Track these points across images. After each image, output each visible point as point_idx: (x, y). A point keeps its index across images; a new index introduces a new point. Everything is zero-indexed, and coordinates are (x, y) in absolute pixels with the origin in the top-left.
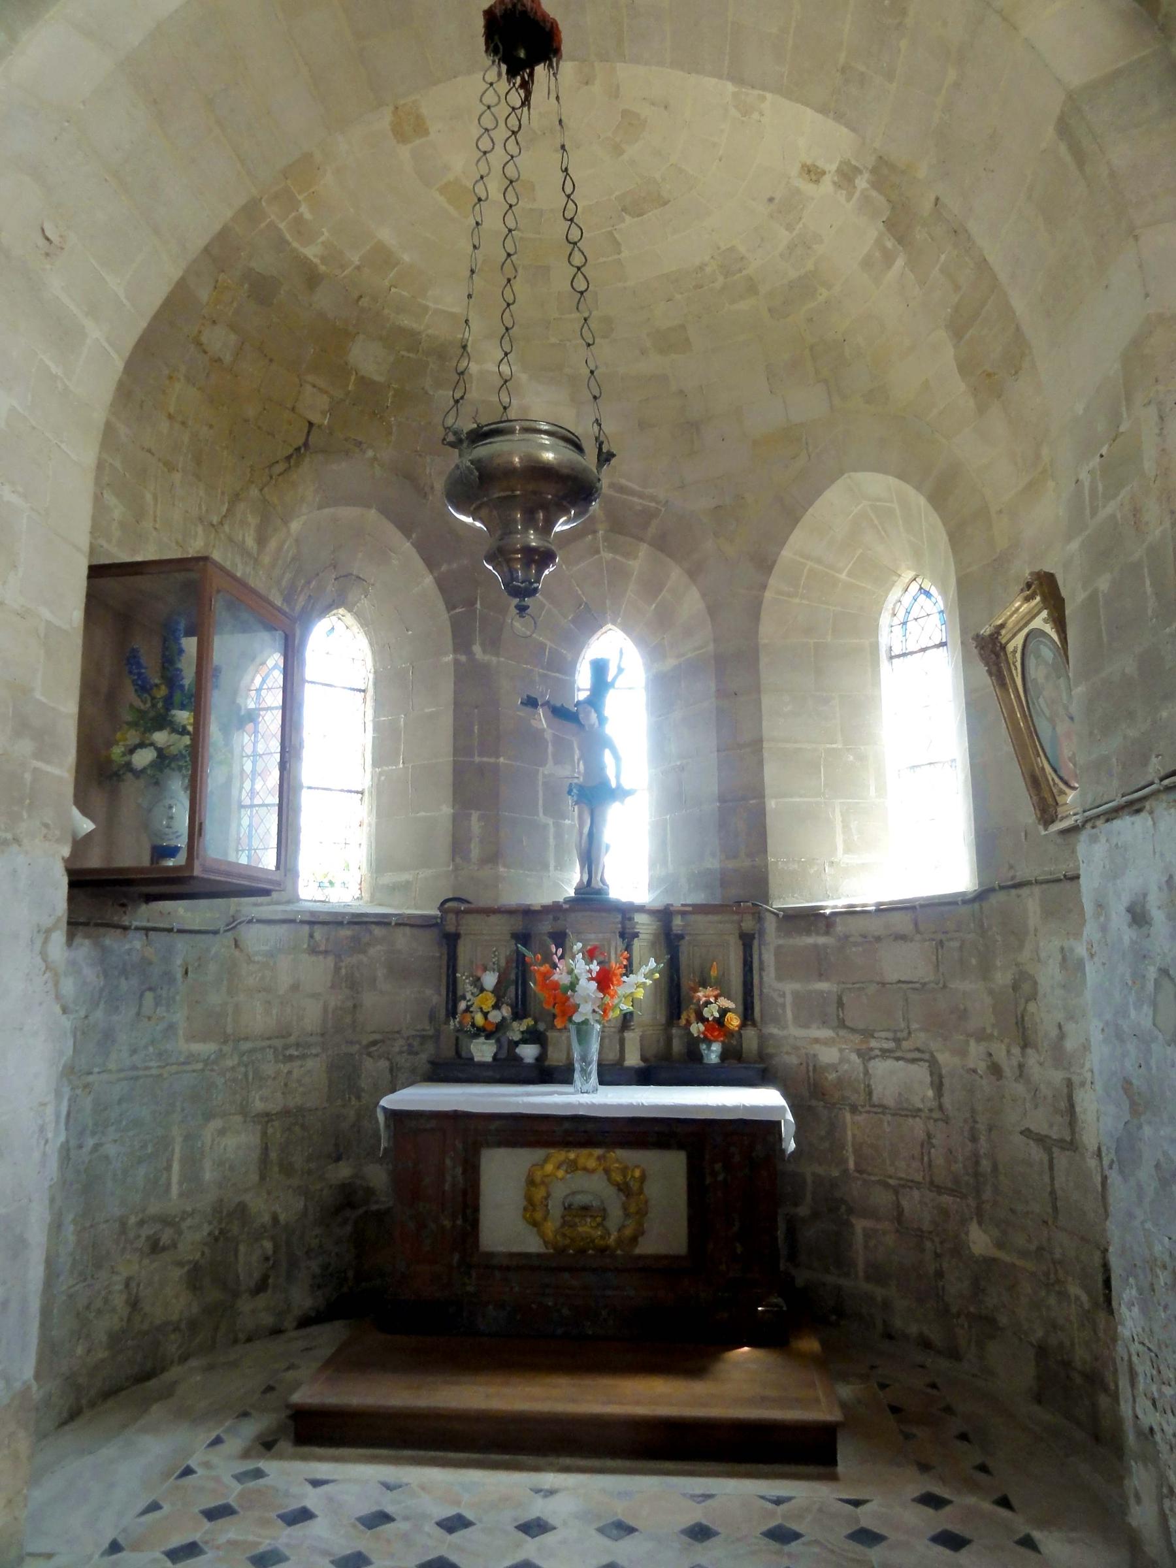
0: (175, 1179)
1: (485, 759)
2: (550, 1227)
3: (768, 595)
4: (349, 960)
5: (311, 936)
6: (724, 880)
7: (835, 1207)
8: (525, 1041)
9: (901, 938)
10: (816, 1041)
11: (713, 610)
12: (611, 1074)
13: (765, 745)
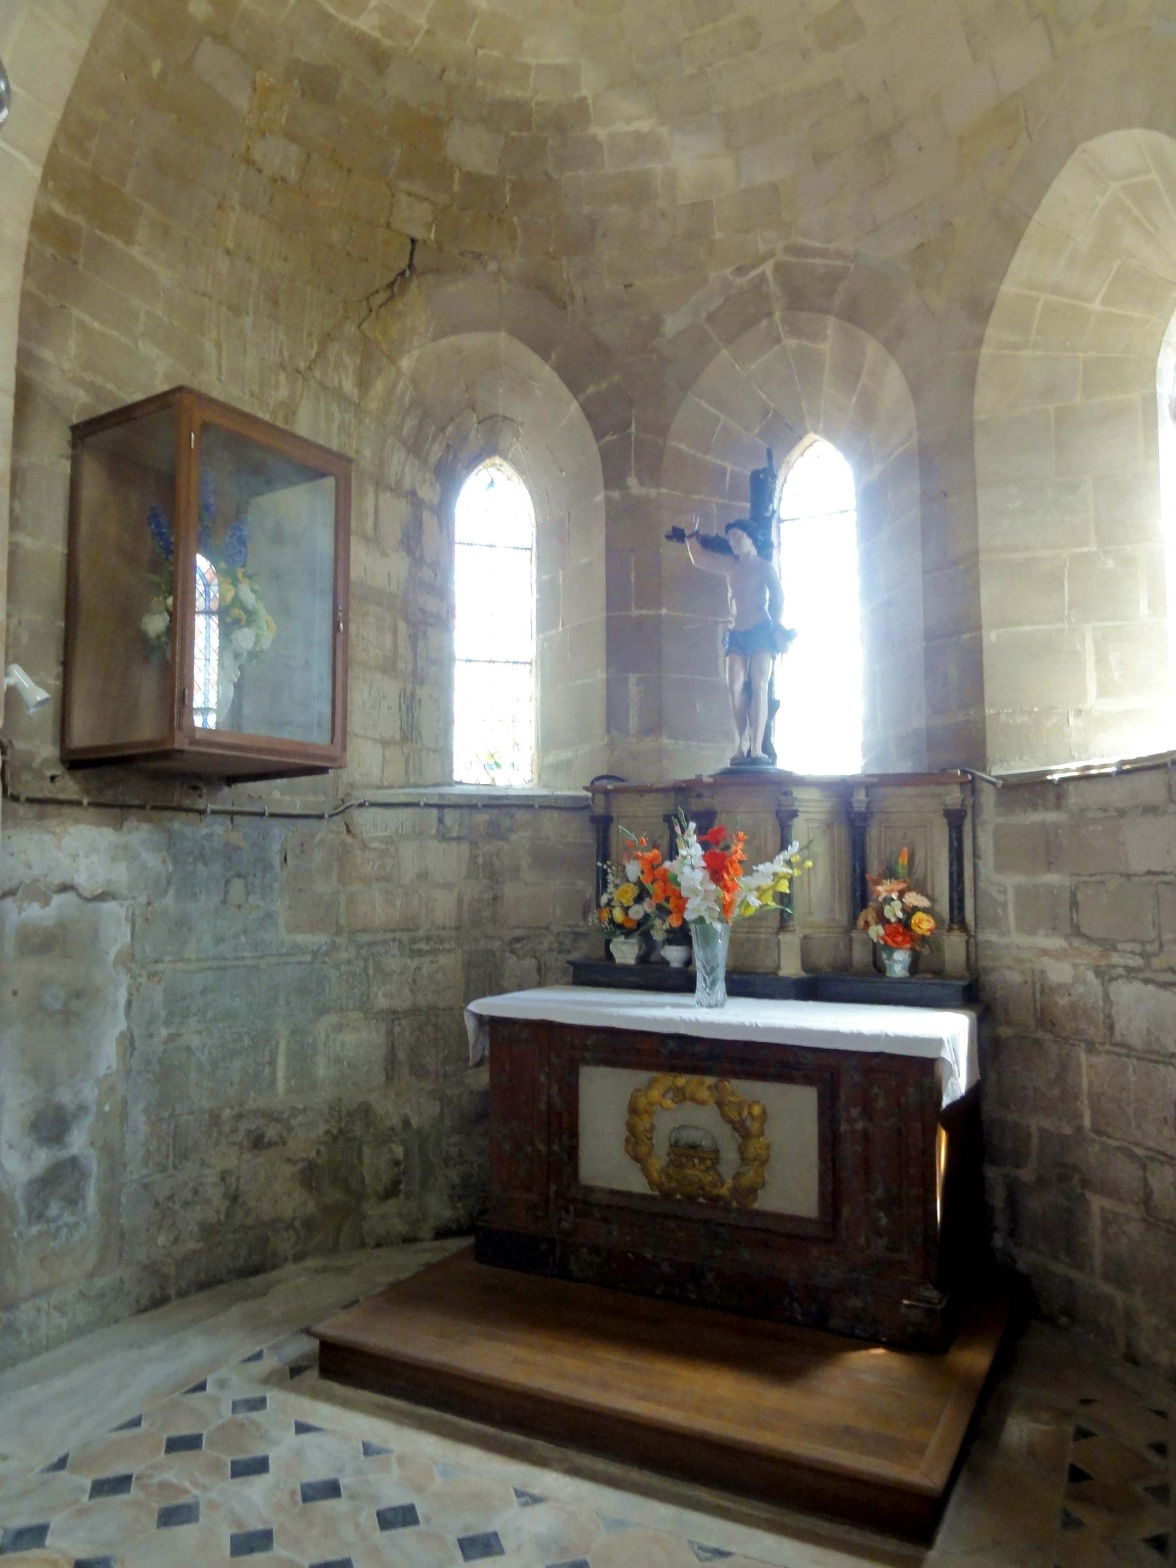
0: (280, 1074)
1: (644, 612)
3: (986, 351)
4: (487, 847)
5: (441, 821)
6: (932, 742)
7: (1066, 1175)
8: (669, 942)
9: (1151, 810)
10: (1045, 952)
11: (916, 389)
13: (983, 557)
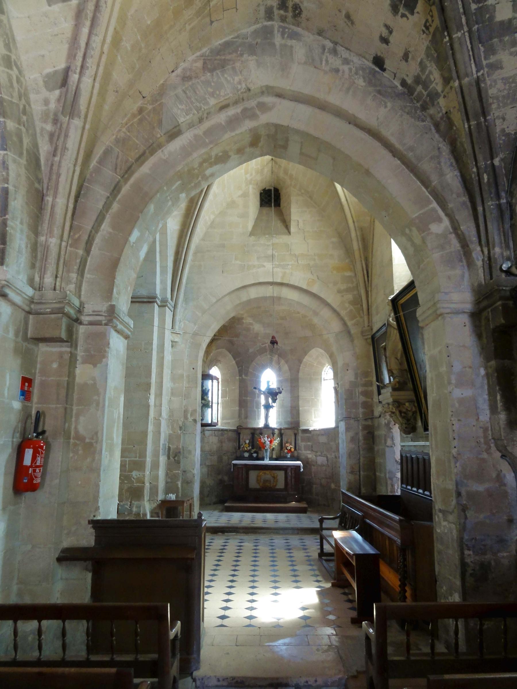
2: (261, 484)
3: (301, 368)
6: (291, 423)
9: (322, 435)
11: (290, 370)
12: (271, 459)
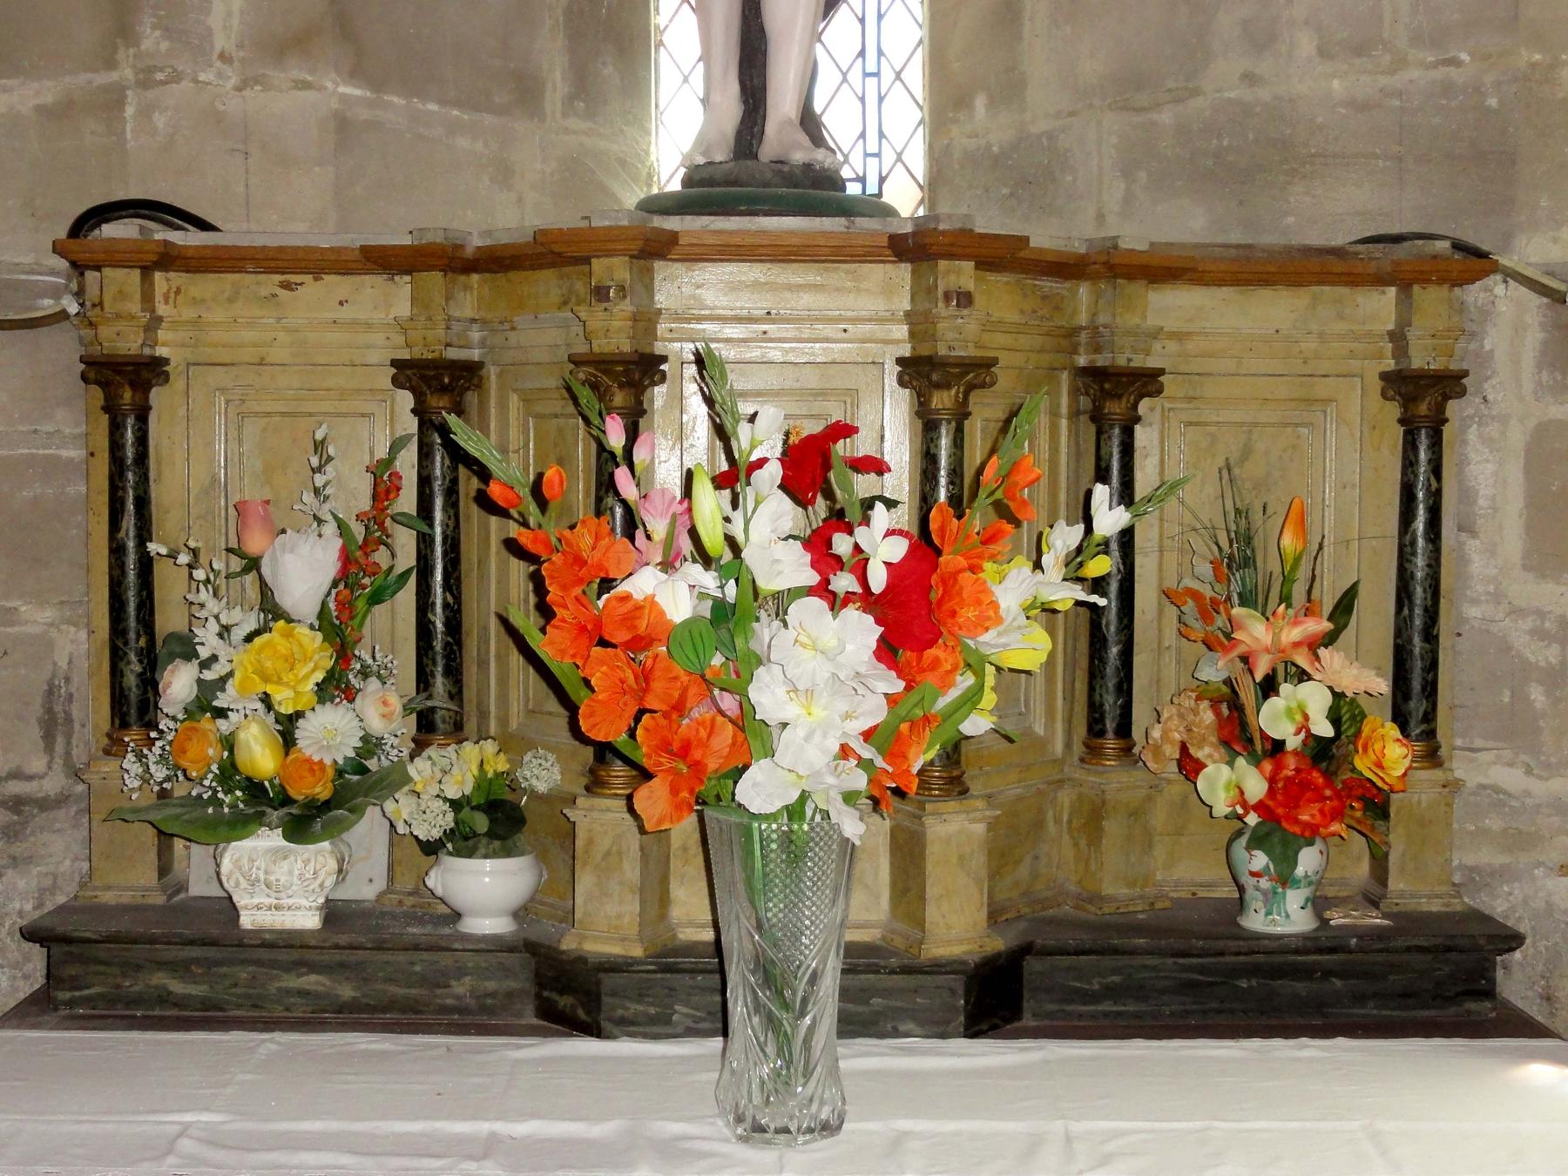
8: (461, 841)
